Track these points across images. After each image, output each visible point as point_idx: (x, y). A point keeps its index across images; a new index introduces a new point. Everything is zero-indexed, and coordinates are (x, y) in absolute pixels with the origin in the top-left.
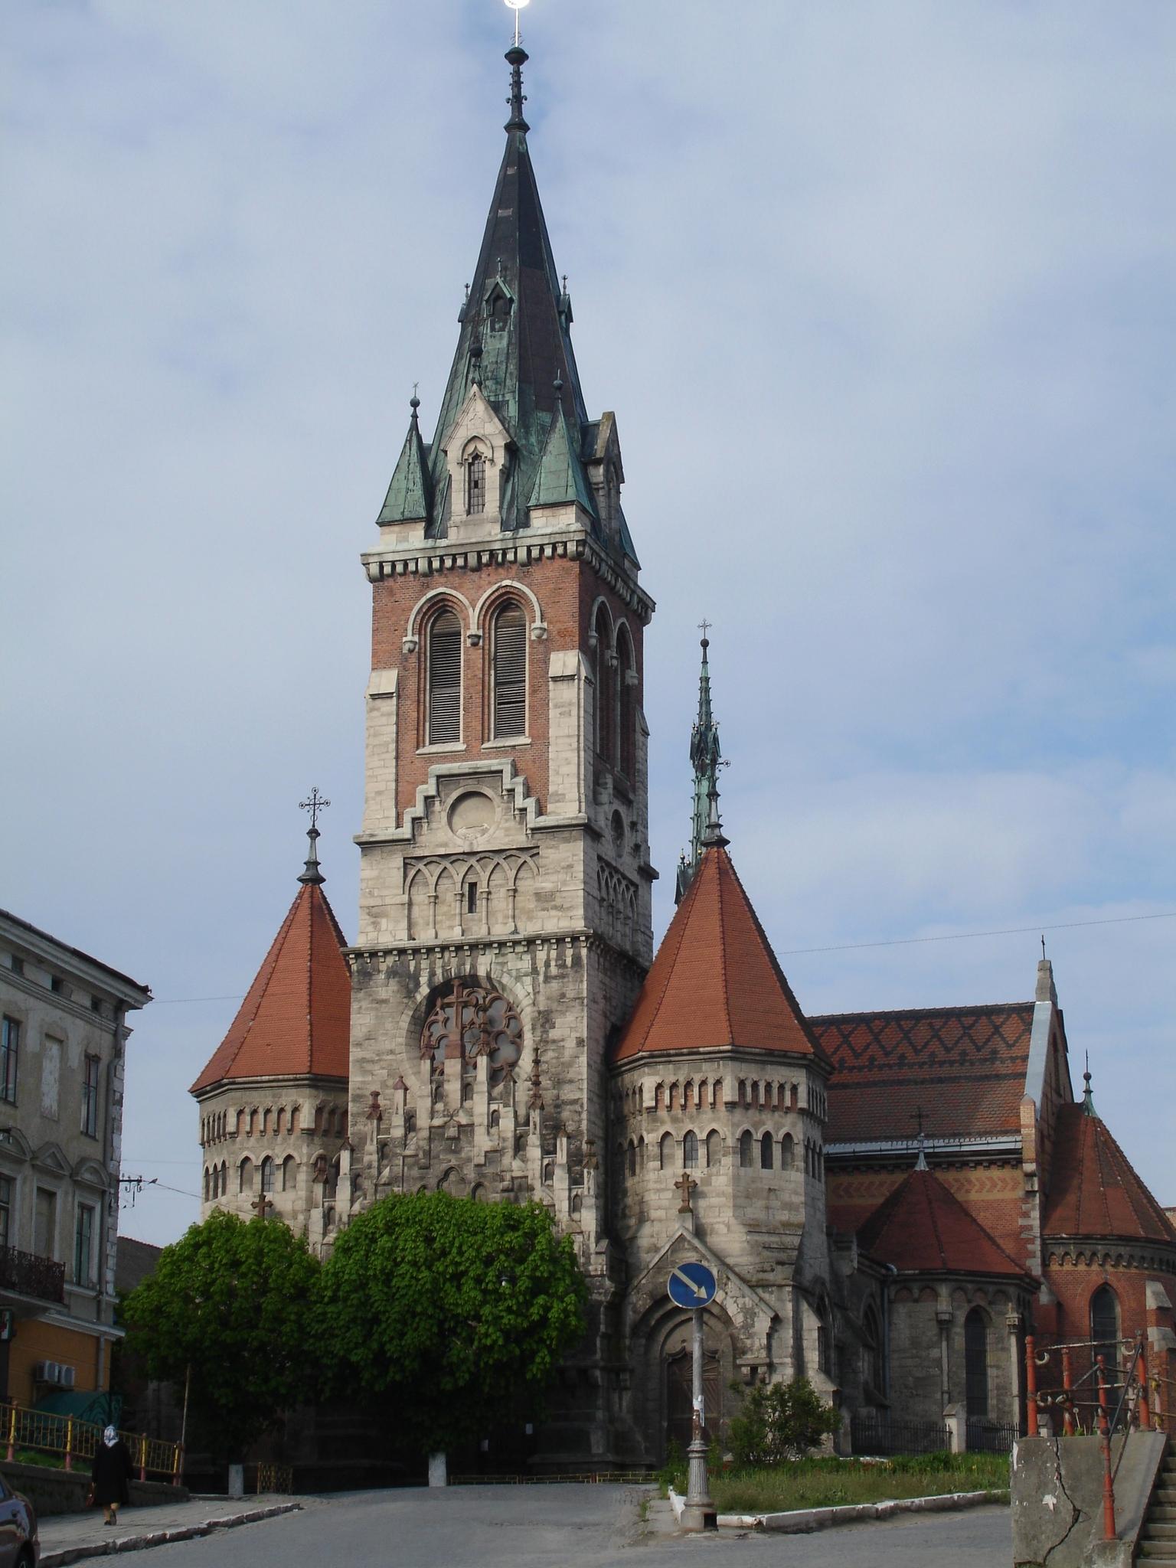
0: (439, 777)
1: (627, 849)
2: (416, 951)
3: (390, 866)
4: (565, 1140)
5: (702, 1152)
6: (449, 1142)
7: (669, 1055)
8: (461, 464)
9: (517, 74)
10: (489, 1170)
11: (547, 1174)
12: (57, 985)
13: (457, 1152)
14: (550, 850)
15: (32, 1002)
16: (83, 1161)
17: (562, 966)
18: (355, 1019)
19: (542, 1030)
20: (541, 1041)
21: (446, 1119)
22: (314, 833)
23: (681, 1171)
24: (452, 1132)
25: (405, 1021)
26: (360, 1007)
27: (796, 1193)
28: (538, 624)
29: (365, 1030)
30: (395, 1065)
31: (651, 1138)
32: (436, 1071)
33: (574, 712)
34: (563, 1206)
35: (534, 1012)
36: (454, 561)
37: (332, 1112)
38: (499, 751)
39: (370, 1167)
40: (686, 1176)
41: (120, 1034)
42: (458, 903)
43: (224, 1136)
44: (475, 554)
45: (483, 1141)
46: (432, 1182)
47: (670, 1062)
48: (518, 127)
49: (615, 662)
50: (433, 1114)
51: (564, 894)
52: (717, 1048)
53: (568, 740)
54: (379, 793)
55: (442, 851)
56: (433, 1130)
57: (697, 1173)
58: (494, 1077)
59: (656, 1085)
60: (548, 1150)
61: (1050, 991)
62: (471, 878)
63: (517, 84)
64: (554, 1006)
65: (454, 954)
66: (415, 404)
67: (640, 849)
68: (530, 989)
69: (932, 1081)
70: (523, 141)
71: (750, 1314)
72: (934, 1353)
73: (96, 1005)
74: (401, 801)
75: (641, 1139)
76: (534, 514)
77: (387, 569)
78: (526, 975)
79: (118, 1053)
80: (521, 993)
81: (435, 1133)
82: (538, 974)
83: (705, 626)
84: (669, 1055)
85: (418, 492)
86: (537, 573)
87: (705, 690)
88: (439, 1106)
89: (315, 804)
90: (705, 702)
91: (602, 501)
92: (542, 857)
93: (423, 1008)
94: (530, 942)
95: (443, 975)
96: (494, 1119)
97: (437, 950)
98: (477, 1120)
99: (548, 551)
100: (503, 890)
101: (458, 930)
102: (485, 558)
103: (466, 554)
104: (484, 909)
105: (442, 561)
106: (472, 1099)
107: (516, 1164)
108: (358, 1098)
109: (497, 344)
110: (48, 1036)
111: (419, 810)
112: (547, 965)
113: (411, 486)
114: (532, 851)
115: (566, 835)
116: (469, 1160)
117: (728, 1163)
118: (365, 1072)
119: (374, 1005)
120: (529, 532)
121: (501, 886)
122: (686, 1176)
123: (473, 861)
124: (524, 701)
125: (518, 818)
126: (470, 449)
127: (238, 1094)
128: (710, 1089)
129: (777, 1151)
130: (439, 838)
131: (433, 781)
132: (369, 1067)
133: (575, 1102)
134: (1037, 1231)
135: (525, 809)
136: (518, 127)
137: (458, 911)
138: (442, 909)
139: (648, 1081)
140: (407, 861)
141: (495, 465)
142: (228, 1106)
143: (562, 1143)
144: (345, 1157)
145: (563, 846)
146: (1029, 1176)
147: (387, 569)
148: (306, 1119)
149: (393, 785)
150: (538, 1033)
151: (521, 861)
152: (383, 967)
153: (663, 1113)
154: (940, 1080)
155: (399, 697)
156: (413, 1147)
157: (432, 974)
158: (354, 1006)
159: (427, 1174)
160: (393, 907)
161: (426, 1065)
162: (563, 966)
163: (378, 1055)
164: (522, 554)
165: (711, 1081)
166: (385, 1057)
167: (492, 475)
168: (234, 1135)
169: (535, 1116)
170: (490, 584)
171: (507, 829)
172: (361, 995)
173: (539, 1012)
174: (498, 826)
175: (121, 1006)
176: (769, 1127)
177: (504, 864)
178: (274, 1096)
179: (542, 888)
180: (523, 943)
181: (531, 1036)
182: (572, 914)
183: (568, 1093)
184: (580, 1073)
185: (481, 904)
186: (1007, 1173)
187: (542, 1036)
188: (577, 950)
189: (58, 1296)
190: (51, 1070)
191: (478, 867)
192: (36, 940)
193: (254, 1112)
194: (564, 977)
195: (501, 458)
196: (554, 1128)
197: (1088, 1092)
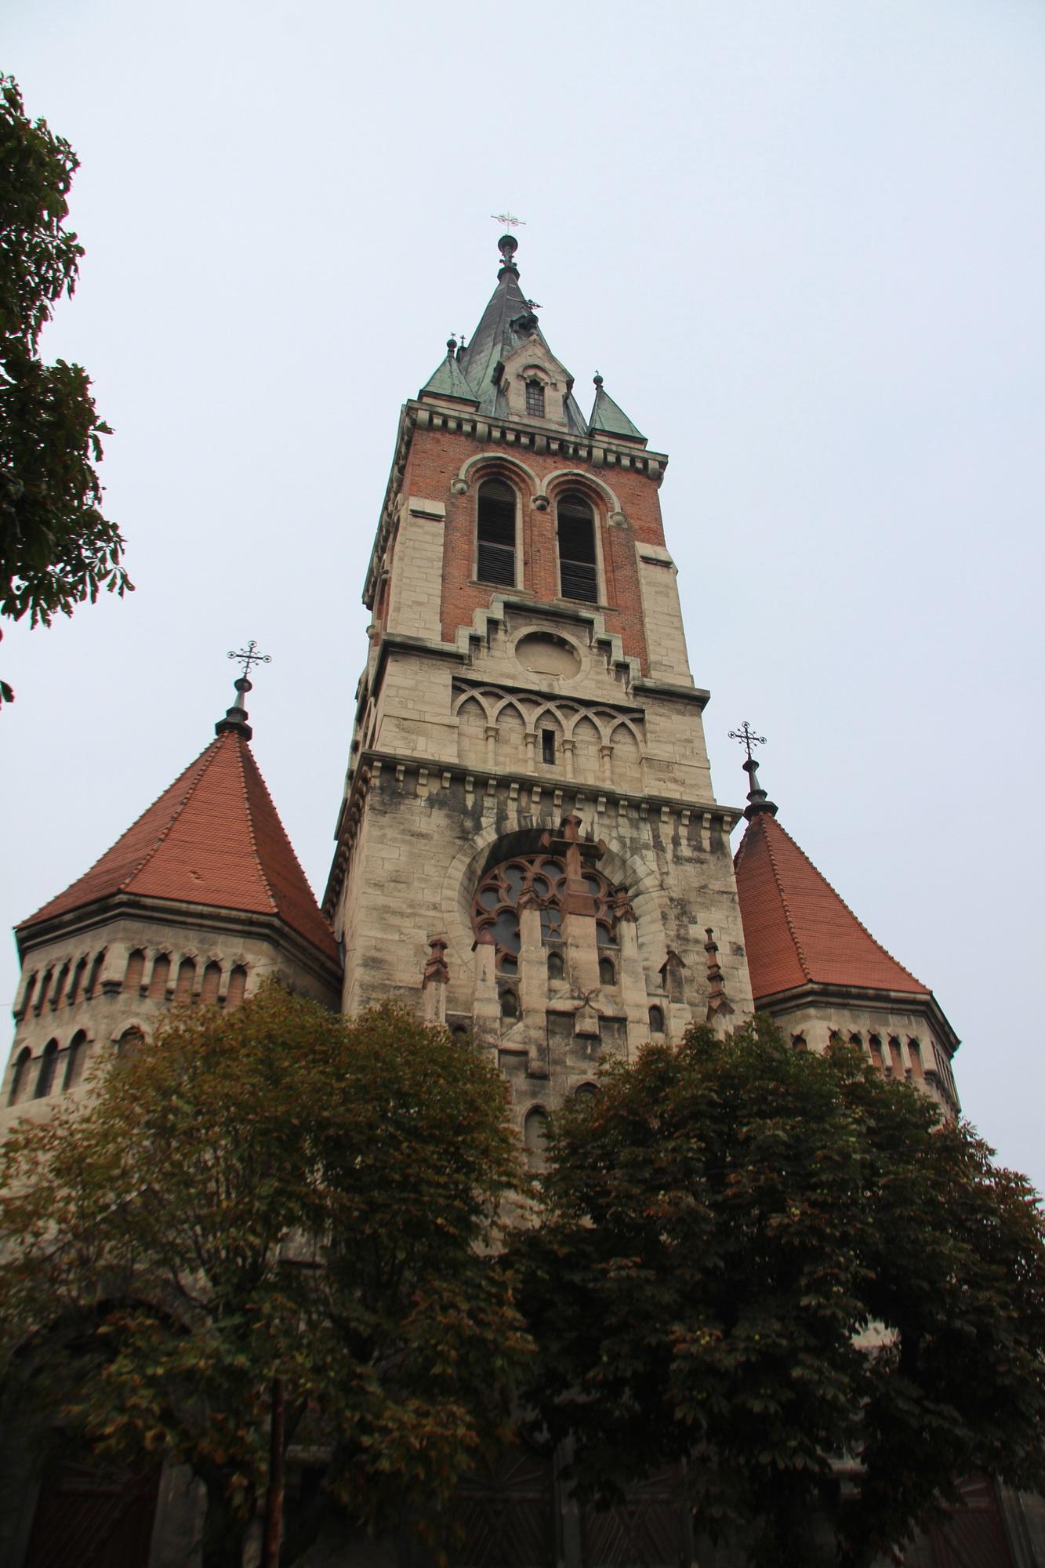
2: (482, 782)
3: (431, 679)
6: (579, 1040)
7: (850, 996)
8: (520, 376)
13: (591, 1058)
14: (658, 718)
17: (699, 848)
19: (677, 922)
20: (678, 937)
21: (577, 1003)
22: (243, 685)
24: (589, 1025)
25: (458, 870)
26: (384, 835)
29: (388, 866)
30: (440, 927)
35: (662, 897)
36: (518, 438)
42: (530, 746)
43: (89, 990)
44: (545, 439)
47: (844, 1006)
48: (509, 273)
50: (551, 992)
51: (683, 768)
52: (912, 996)
53: (668, 617)
55: (509, 683)
56: (552, 1018)
59: (829, 1033)
62: (550, 726)
64: (693, 896)
65: (536, 798)
68: (654, 866)
78: (646, 847)
80: (645, 866)
81: (560, 1020)
82: (663, 850)
84: (850, 996)
88: (556, 983)
89: (250, 657)
92: (650, 722)
93: (482, 861)
94: (651, 808)
95: (519, 821)
97: (515, 786)
98: (631, 1014)
100: (593, 750)
102: (555, 446)
104: (569, 761)
106: (613, 983)
111: (481, 629)
112: (676, 842)
113: (457, 382)
115: (680, 707)
118: (388, 927)
119: (408, 838)
121: (590, 743)
123: (551, 706)
124: (594, 580)
125: (613, 674)
126: (531, 372)
127: (137, 925)
132: (395, 920)
135: (622, 667)
136: (509, 273)
137: (530, 754)
140: (458, 684)
141: (557, 390)
142: (110, 941)
145: (675, 717)
147: (438, 421)
149: (438, 601)
150: (673, 924)
151: (617, 722)
155: (446, 527)
156: (518, 1038)
157: (502, 817)
159: (543, 1087)
160: (436, 726)
162: (699, 848)
163: (411, 906)
166: (423, 912)
168: (113, 988)
170: (556, 468)
171: (598, 682)
172: (385, 820)
173: (671, 899)
174: (587, 675)
177: (595, 719)
178: (202, 941)
179: (655, 755)
180: (643, 806)
181: (662, 928)
182: (697, 793)
184: (741, 991)
187: (678, 930)
188: (716, 834)
191: (558, 714)
193: (163, 959)
194: (702, 863)
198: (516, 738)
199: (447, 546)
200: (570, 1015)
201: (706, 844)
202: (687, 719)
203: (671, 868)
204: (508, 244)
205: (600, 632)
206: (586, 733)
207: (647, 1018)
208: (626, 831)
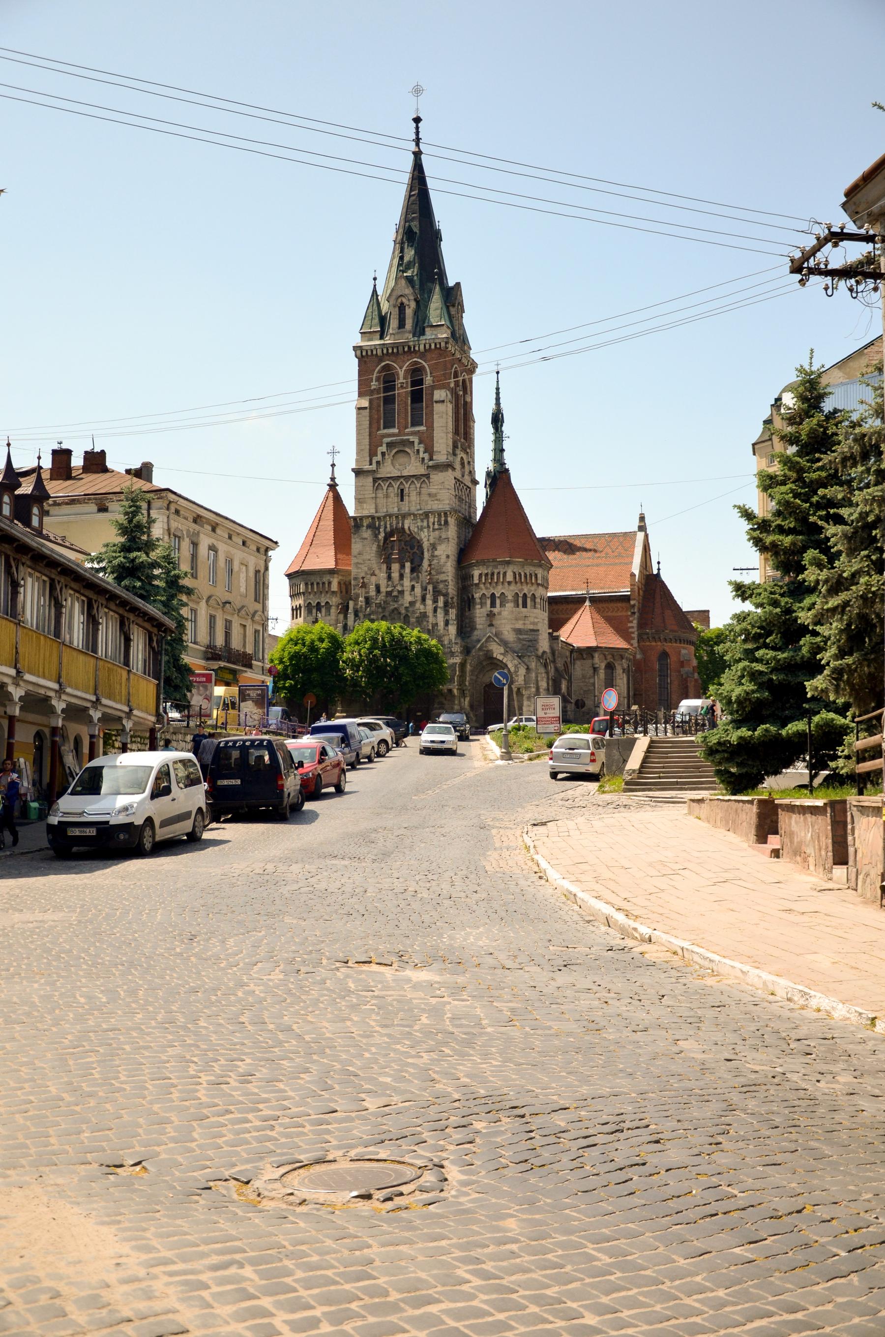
0: (387, 444)
1: (467, 473)
2: (379, 518)
4: (442, 598)
5: (498, 602)
9: (417, 128)
10: (410, 609)
11: (435, 610)
12: (244, 543)
15: (235, 551)
16: (256, 612)
17: (440, 525)
18: (353, 546)
20: (433, 556)
22: (333, 465)
23: (489, 609)
24: (395, 593)
25: (374, 547)
27: (536, 618)
28: (429, 378)
31: (477, 596)
32: (389, 568)
33: (444, 416)
34: (441, 624)
37: (345, 583)
38: (413, 433)
39: (361, 607)
40: (491, 611)
41: (267, 562)
45: (408, 598)
46: (387, 614)
49: (461, 393)
50: (388, 586)
54: (362, 450)
55: (389, 475)
57: (496, 610)
58: (413, 570)
60: (435, 601)
61: (642, 528)
62: (402, 487)
63: (417, 133)
64: (437, 542)
66: (375, 279)
67: (472, 473)
69: (593, 565)
70: (420, 159)
71: (516, 666)
72: (592, 681)
73: (258, 550)
74: (372, 453)
75: (473, 596)
76: (427, 329)
77: (364, 353)
79: (267, 569)
81: (389, 594)
83: (498, 365)
85: (376, 320)
86: (428, 355)
87: (498, 394)
88: (390, 583)
89: (333, 452)
90: (498, 399)
91: (456, 323)
93: (382, 542)
94: (426, 515)
96: (413, 588)
98: (405, 589)
99: (433, 346)
101: (396, 509)
102: (406, 349)
103: (397, 348)
105: (388, 350)
107: (422, 607)
108: (355, 579)
109: (410, 254)
110: (242, 564)
111: (379, 458)
112: (434, 524)
114: (428, 476)
116: (402, 605)
117: (510, 605)
118: (358, 568)
120: (425, 337)
122: (491, 611)
123: (402, 480)
126: (399, 300)
128: (501, 576)
129: (529, 600)
130: (388, 470)
131: (384, 445)
133: (446, 581)
134: (635, 629)
135: (423, 459)
136: (417, 155)
138: (390, 500)
139: (476, 573)
143: (441, 600)
144: (351, 604)
145: (440, 474)
146: (634, 606)
147: (364, 353)
148: (335, 587)
152: (365, 524)
153: (482, 586)
154: (597, 565)
157: (386, 527)
158: (353, 540)
161: (384, 566)
162: (440, 525)
164: (422, 347)
165: (502, 573)
167: (409, 312)
168: (303, 593)
169: (430, 587)
170: (408, 360)
175: (267, 550)
176: (526, 591)
183: (442, 577)
185: (406, 498)
186: (624, 605)
189: (250, 666)
190: (243, 576)
192: (237, 527)
193: (312, 584)
195: (413, 305)
196: (437, 593)
197: (659, 569)
198: (392, 495)
199: (370, 417)
200: (391, 592)
201: (443, 523)
202: (444, 474)
203: (431, 533)
204: (417, 120)
205: (416, 448)
206: (413, 486)
207: (409, 589)
208: (419, 524)
